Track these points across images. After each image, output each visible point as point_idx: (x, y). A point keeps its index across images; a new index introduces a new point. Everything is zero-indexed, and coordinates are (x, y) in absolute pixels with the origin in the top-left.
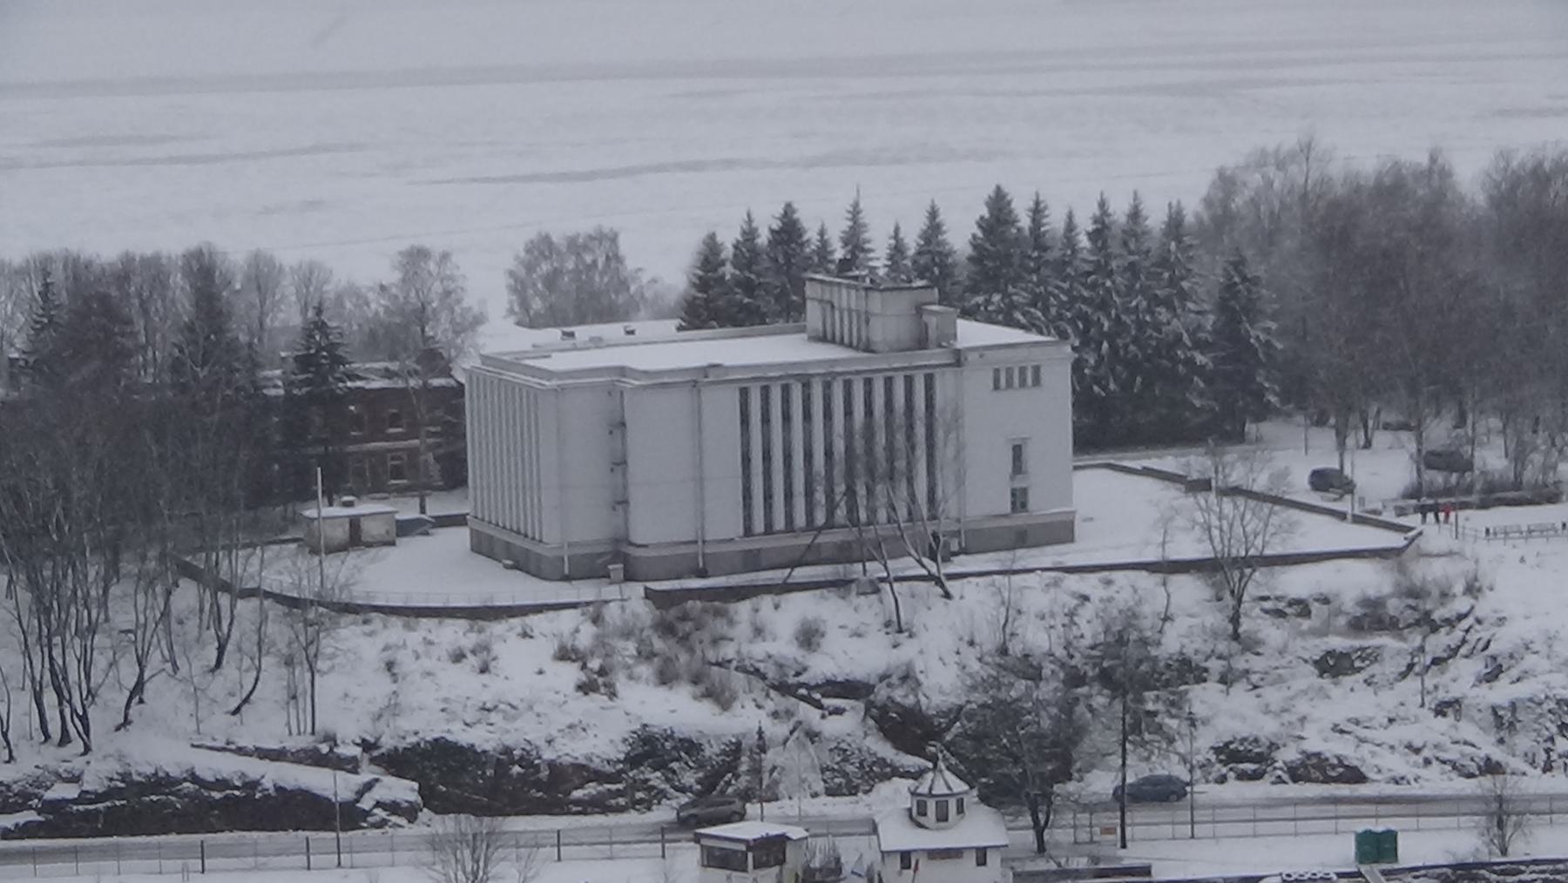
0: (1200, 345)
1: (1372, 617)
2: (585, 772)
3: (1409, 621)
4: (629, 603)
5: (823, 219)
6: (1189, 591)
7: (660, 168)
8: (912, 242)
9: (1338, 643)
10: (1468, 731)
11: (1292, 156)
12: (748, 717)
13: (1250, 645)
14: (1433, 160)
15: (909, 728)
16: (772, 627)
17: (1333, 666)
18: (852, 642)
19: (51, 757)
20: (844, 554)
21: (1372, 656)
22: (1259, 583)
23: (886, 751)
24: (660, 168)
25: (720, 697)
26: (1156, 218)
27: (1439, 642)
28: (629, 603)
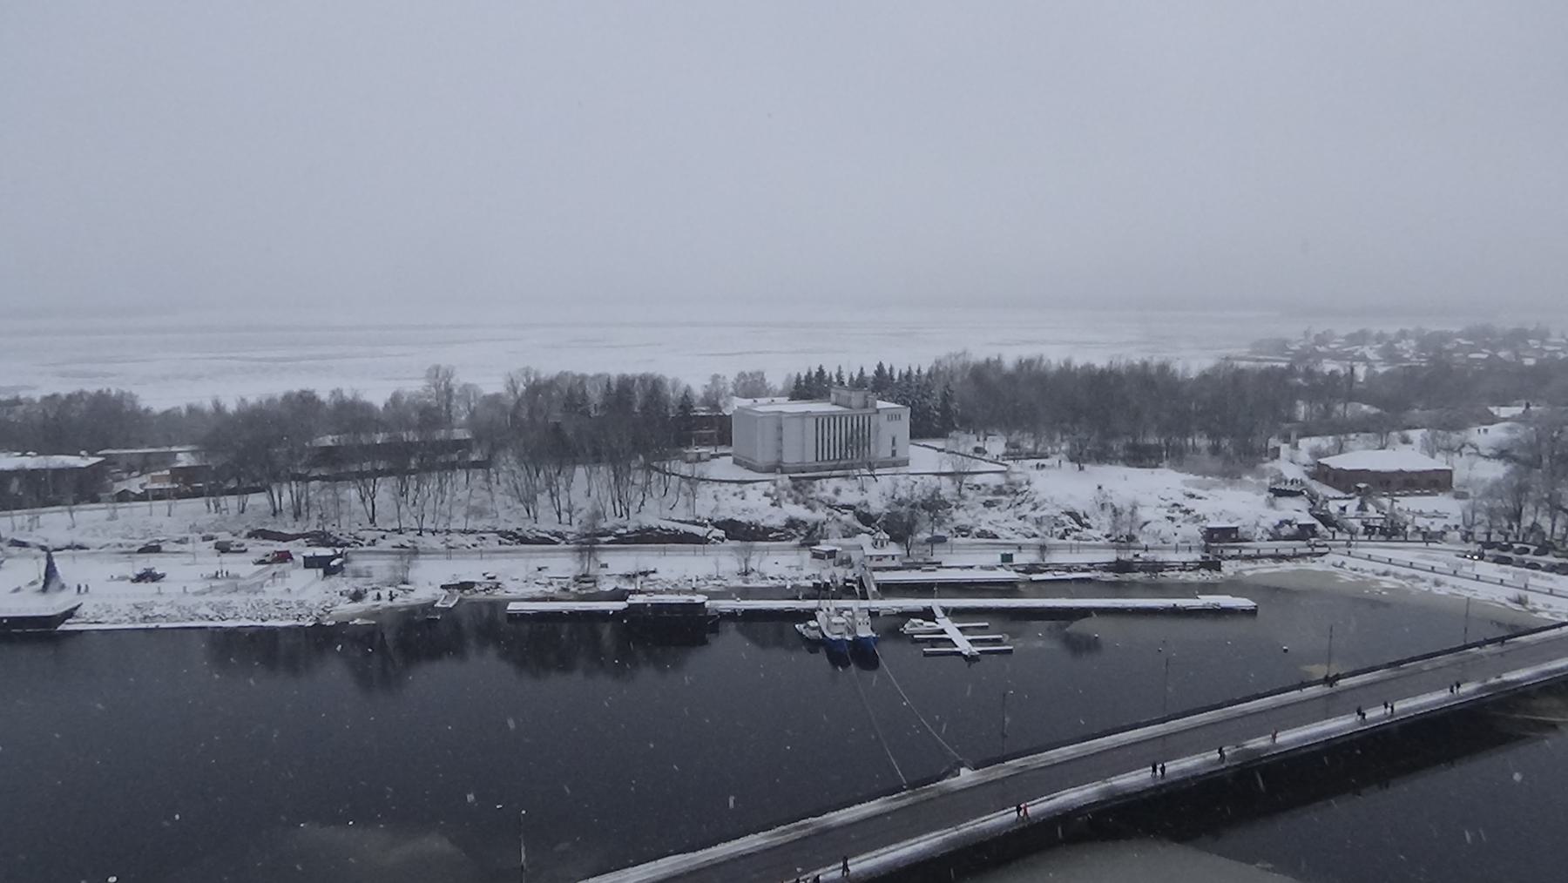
1: (999, 491)
2: (772, 530)
3: (1011, 491)
4: (783, 480)
5: (830, 370)
6: (946, 481)
8: (855, 376)
9: (990, 498)
10: (1028, 525)
12: (820, 515)
13: (963, 497)
15: (867, 519)
16: (826, 488)
18: (849, 495)
19: (618, 520)
20: (844, 468)
21: (999, 502)
22: (966, 480)
23: (860, 525)
25: (812, 508)
26: (925, 371)
27: (1019, 498)
28: (783, 480)
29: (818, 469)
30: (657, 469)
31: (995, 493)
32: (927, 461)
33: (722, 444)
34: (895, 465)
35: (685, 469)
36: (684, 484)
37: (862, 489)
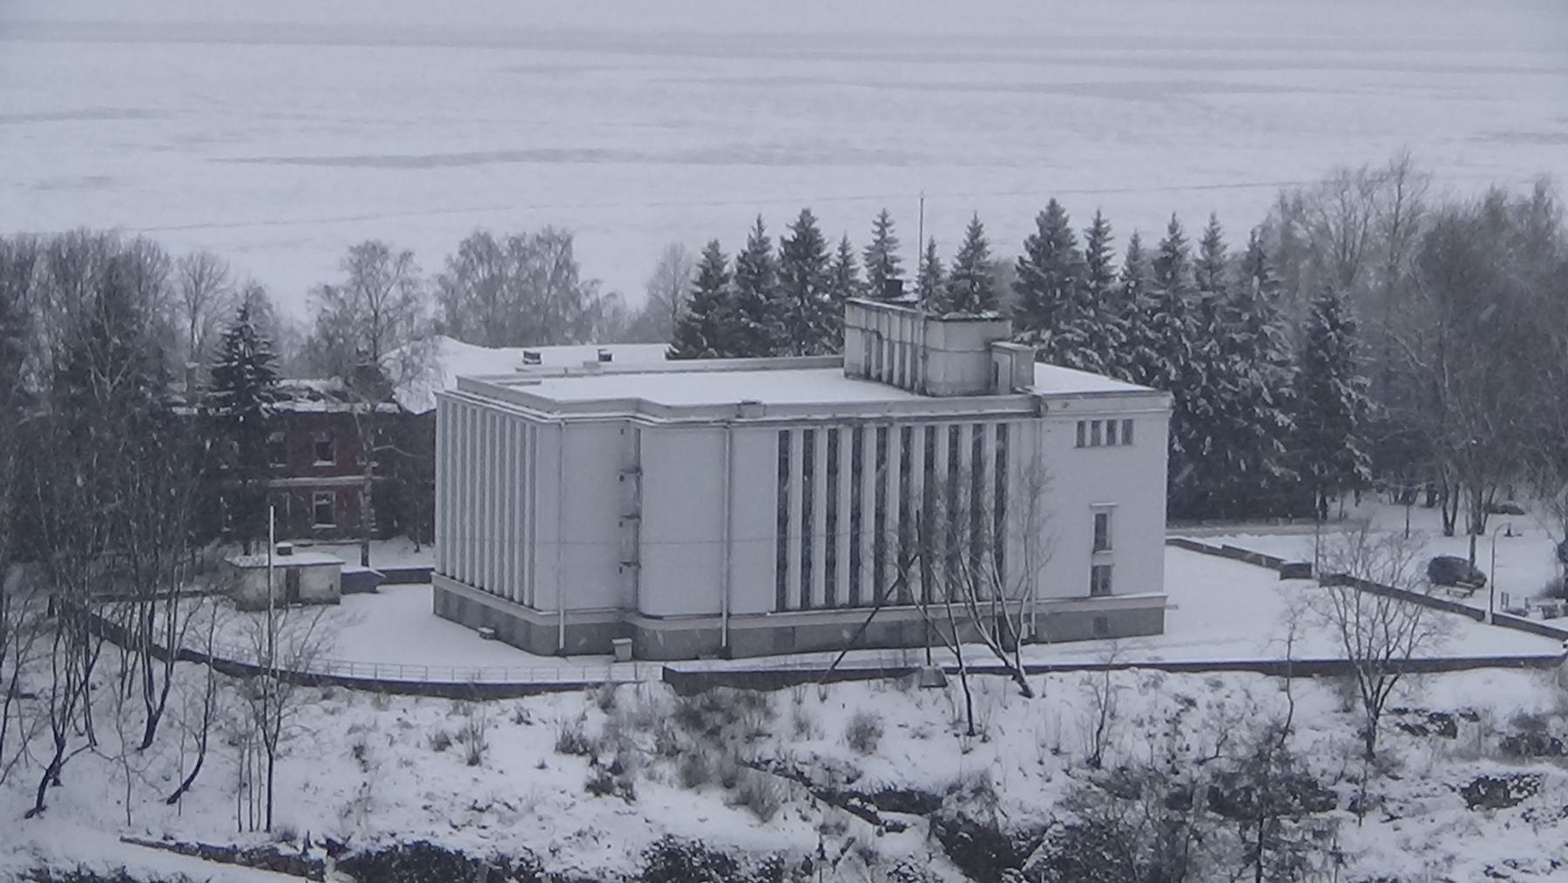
0: (1280, 402)
1: (1530, 739)
4: (645, 686)
5: (846, 232)
6: (1313, 698)
7: (509, 156)
8: (948, 262)
9: (1492, 768)
11: (1381, 179)
13: (1386, 767)
14: (1540, 193)
16: (816, 723)
17: (1485, 795)
21: (1531, 786)
24: (509, 156)
25: (758, 805)
26: (1236, 243)
28: (645, 686)
29: (785, 642)
30: (117, 636)
31: (1511, 749)
32: (1232, 603)
33: (386, 535)
34: (1103, 628)
35: (233, 635)
36: (230, 700)
37: (971, 730)
